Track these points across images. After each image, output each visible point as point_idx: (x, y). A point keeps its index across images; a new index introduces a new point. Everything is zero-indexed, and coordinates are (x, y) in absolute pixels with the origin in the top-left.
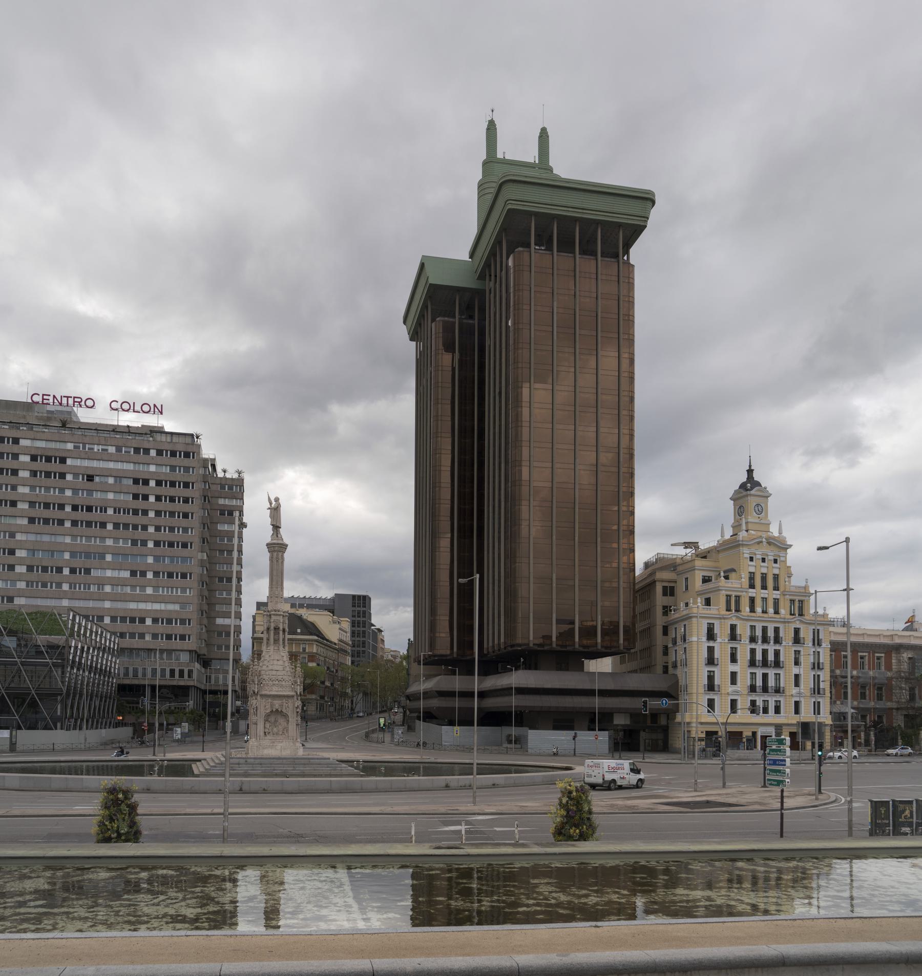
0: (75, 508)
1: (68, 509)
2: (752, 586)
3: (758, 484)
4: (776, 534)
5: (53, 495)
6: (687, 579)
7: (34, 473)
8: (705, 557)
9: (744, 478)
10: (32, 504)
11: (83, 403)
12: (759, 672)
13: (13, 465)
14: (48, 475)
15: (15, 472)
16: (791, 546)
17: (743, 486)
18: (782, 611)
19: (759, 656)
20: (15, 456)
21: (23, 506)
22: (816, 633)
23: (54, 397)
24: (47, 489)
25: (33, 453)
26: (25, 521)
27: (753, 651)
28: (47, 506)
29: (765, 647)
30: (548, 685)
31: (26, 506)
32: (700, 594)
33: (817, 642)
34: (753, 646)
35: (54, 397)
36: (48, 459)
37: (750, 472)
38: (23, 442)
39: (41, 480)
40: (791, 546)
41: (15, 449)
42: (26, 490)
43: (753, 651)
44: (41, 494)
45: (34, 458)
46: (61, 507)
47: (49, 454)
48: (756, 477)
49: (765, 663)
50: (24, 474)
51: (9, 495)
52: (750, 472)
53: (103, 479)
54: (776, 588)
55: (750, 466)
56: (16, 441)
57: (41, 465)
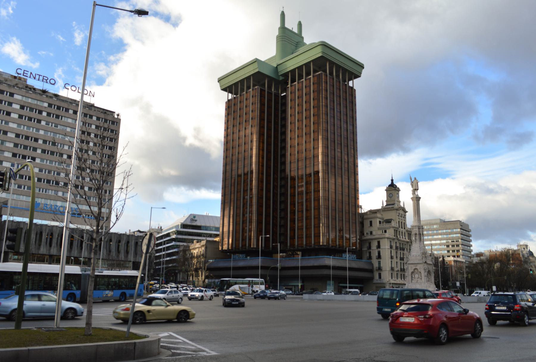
0: (45, 142)
1: (40, 142)
4: (402, 206)
5: (32, 132)
6: (371, 222)
7: (21, 117)
9: (390, 183)
10: (17, 136)
11: (48, 81)
13: (9, 109)
14: (30, 119)
15: (8, 114)
17: (389, 186)
20: (10, 104)
21: (11, 135)
23: (31, 73)
24: (29, 127)
25: (22, 104)
26: (11, 145)
28: (27, 138)
31: (13, 136)
32: (379, 229)
35: (31, 73)
36: (31, 109)
37: (392, 180)
38: (16, 96)
39: (25, 121)
41: (11, 99)
42: (14, 126)
44: (24, 130)
45: (22, 107)
46: (36, 140)
47: (33, 107)
50: (14, 116)
51: (3, 126)
52: (392, 180)
53: (62, 127)
56: (12, 95)
57: (26, 112)
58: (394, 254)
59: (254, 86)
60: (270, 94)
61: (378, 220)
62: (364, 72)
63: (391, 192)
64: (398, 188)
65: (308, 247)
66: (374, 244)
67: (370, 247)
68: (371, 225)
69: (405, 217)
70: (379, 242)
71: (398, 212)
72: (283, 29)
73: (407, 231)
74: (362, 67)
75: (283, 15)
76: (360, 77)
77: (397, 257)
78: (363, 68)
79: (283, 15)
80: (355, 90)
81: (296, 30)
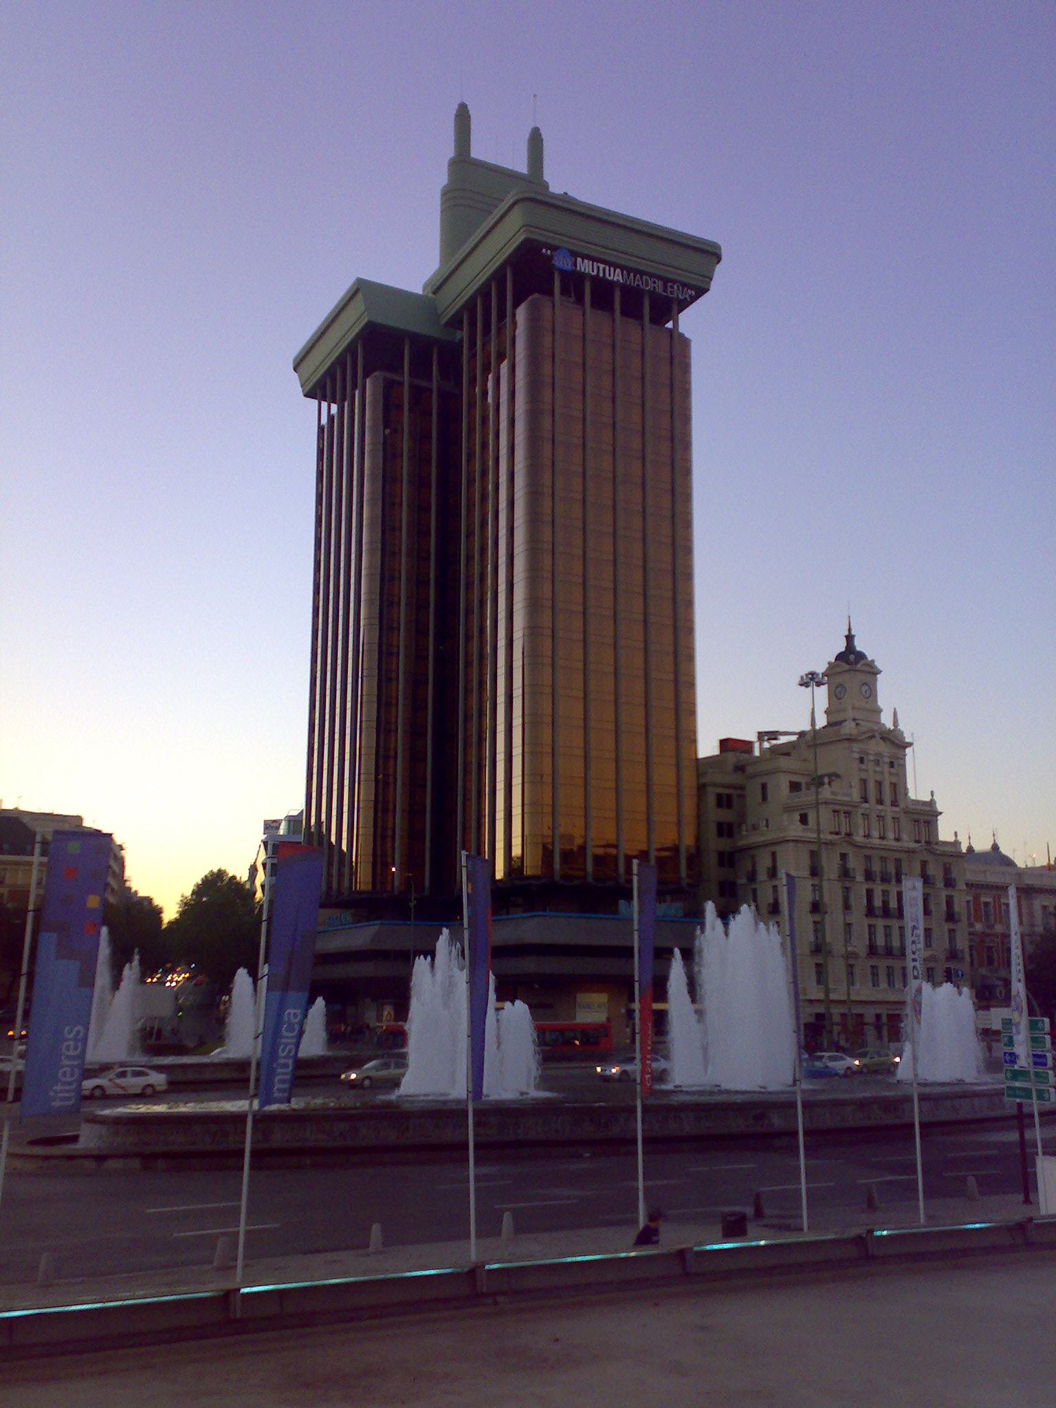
2: (865, 800)
3: (861, 656)
6: (764, 786)
8: (788, 754)
9: (841, 646)
12: (880, 923)
16: (910, 744)
17: (840, 657)
18: (905, 837)
19: (878, 902)
22: (947, 870)
27: (870, 893)
29: (885, 887)
30: (582, 940)
32: (788, 809)
33: (949, 883)
34: (869, 885)
37: (850, 638)
40: (910, 744)
43: (870, 893)
48: (859, 646)
49: (886, 912)
52: (850, 638)
54: (894, 803)
55: (850, 630)
58: (832, 893)
59: (366, 374)
60: (419, 395)
61: (783, 782)
62: (721, 274)
63: (839, 679)
64: (871, 664)
65: (518, 882)
66: (764, 862)
67: (752, 877)
68: (764, 798)
69: (897, 764)
70: (774, 855)
71: (856, 747)
72: (463, 163)
73: (907, 812)
74: (711, 254)
75: (463, 117)
76: (707, 290)
77: (847, 907)
78: (719, 259)
79: (463, 117)
80: (685, 342)
81: (522, 167)
